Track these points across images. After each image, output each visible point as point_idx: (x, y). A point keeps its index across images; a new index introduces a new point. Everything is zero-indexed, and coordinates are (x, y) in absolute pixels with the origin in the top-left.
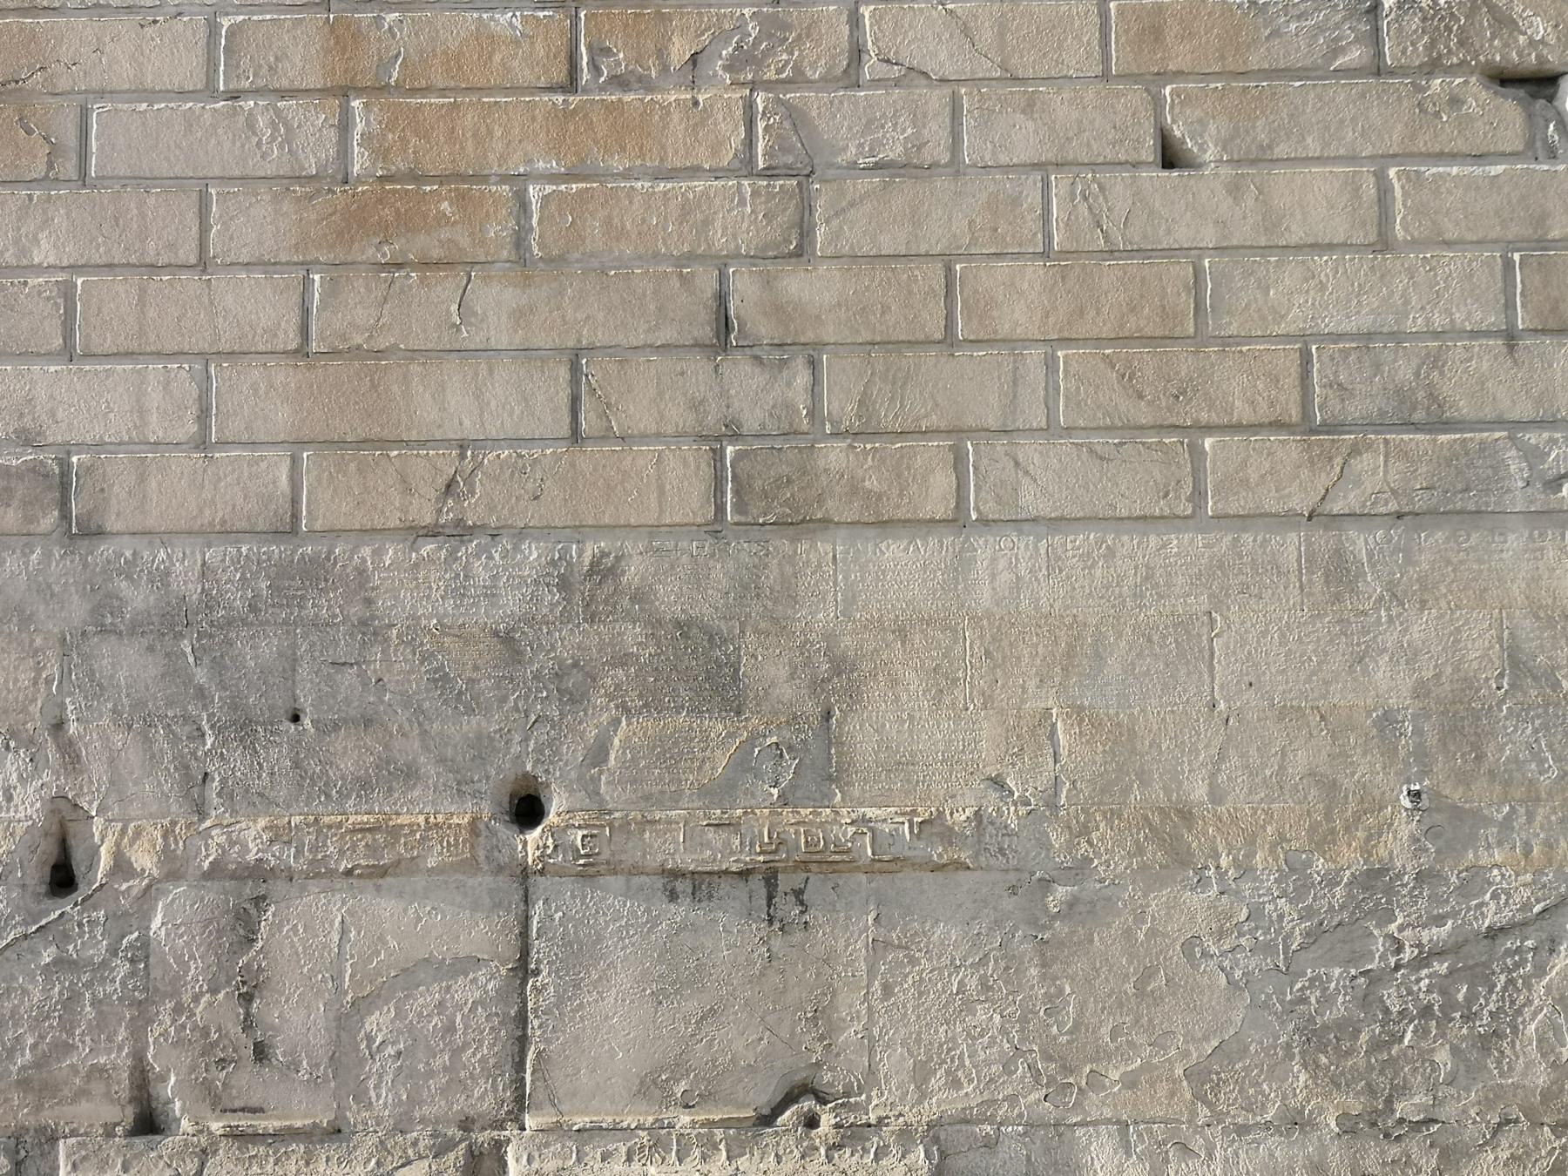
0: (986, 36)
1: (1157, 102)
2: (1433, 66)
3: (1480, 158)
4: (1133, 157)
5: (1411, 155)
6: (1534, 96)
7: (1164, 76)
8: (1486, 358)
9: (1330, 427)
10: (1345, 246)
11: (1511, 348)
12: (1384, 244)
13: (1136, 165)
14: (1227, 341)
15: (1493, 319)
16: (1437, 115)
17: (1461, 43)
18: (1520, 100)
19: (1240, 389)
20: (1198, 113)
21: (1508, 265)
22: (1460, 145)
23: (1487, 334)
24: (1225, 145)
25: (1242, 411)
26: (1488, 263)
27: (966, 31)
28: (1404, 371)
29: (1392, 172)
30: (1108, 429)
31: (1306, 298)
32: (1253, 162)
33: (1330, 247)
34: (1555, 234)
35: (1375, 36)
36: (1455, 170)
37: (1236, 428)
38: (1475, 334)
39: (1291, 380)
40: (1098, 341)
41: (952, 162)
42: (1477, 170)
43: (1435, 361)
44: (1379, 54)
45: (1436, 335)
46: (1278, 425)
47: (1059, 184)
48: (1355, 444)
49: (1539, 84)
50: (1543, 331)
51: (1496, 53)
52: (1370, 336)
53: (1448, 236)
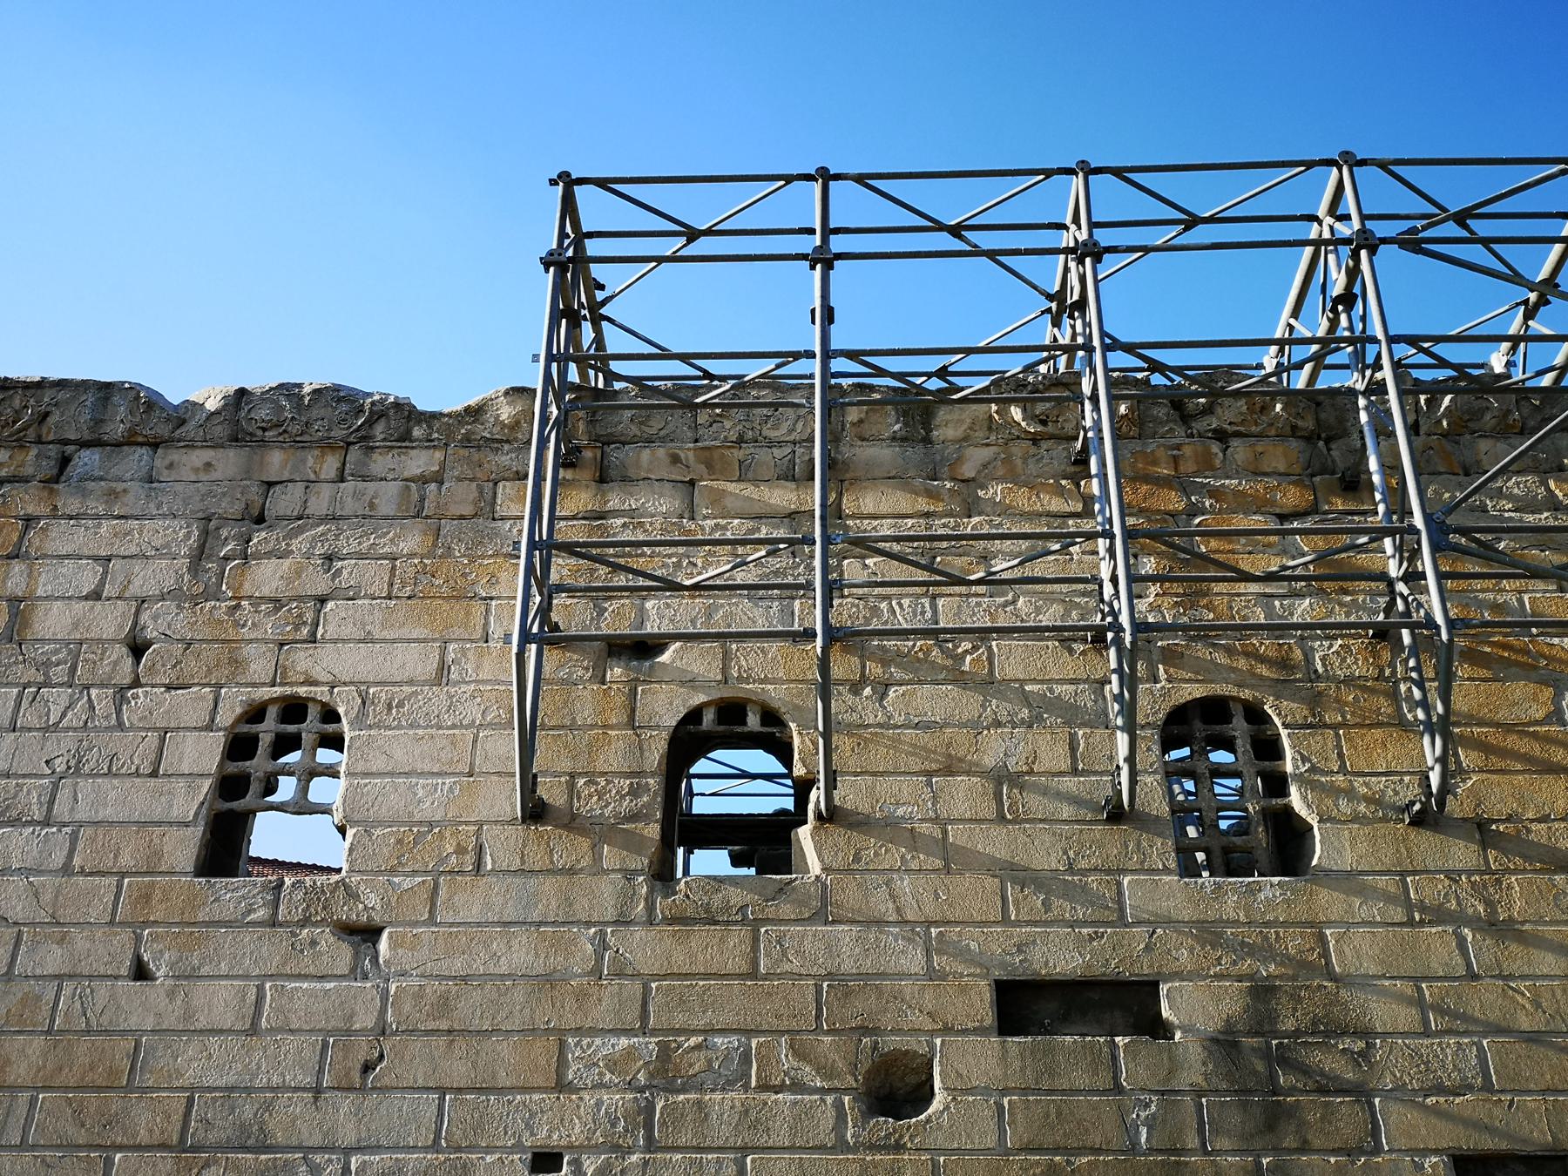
0: (47, 897)
1: (138, 939)
2: (305, 922)
3: (322, 978)
4: (116, 972)
5: (281, 975)
6: (365, 941)
7: (146, 924)
8: (299, 1105)
9: (195, 1149)
10: (230, 1031)
11: (316, 1099)
12: (253, 1030)
13: (116, 978)
14: (145, 1090)
15: (309, 1080)
16: (302, 951)
17: (324, 908)
18: (352, 944)
19: (146, 1121)
20: (161, 946)
21: (325, 1045)
22: (312, 970)
23: (304, 1089)
24: (172, 966)
25: (143, 1137)
26: (313, 1045)
27: (36, 895)
28: (248, 1111)
29: (268, 985)
30: (58, 1147)
31: (197, 1065)
32: (187, 978)
33: (221, 1031)
34: (357, 1026)
35: (276, 904)
36: (306, 985)
37: (138, 1148)
38: (296, 1089)
39: (177, 1118)
40: (67, 1089)
41: (7, 973)
42: (319, 985)
43: (268, 1107)
44: (275, 913)
45: (272, 1089)
46: (163, 1147)
47: (68, 988)
48: (208, 1159)
49: (367, 934)
50: (338, 1089)
51: (344, 913)
52: (232, 1089)
53: (293, 1027)
